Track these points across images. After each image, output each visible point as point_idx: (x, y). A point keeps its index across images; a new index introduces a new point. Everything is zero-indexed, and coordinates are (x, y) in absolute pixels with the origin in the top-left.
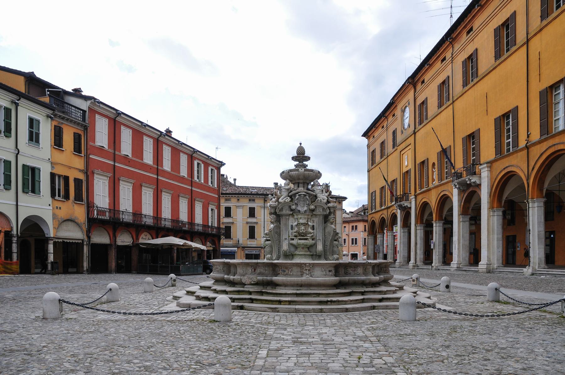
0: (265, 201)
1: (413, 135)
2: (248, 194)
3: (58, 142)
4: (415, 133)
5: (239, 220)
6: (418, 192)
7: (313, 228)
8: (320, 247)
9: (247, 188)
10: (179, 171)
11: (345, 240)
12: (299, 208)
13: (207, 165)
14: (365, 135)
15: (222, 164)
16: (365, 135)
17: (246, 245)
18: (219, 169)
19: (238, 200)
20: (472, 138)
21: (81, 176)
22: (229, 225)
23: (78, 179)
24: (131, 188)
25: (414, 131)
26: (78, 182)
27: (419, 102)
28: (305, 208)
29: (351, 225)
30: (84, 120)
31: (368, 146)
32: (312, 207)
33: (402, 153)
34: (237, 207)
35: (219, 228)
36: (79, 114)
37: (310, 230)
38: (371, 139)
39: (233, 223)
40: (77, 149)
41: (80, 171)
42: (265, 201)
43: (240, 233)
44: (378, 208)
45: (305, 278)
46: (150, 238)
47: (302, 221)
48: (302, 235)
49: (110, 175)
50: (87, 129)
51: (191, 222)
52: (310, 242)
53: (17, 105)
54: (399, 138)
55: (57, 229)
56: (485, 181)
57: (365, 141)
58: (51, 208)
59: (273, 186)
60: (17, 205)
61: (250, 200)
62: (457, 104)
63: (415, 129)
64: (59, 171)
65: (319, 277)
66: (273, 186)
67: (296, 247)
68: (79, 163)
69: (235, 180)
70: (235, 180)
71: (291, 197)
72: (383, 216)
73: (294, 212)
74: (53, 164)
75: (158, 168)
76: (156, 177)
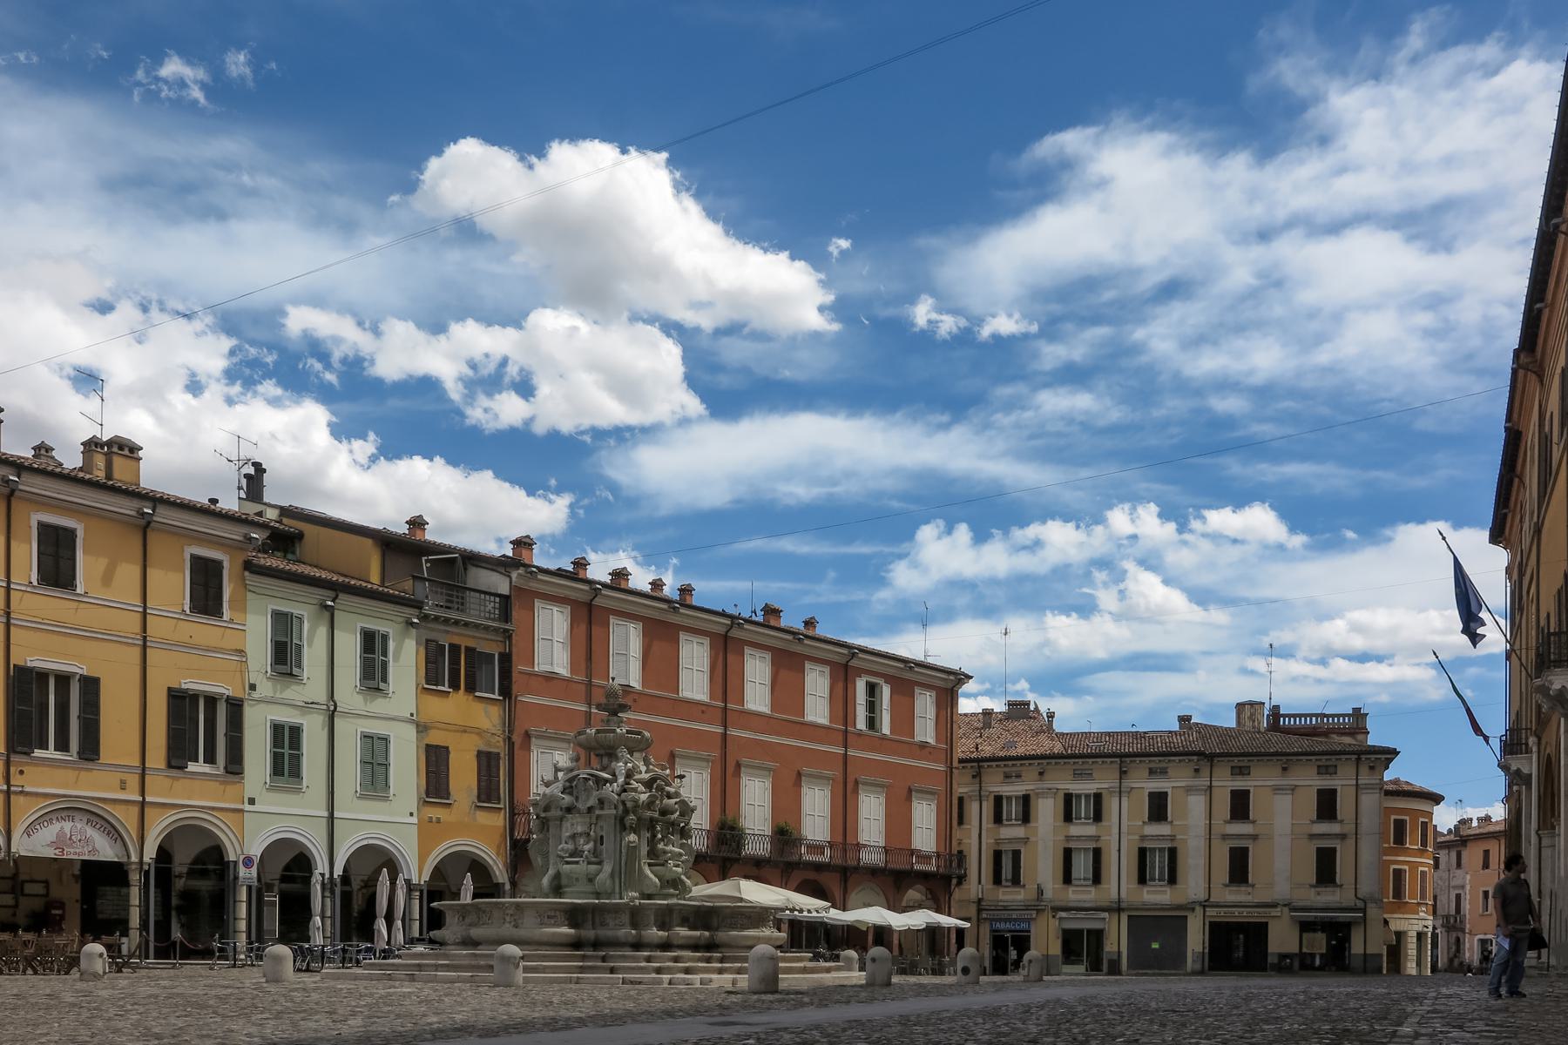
0: (1123, 773)
9: (1137, 736)
19: (1041, 774)
23: (489, 754)
26: (487, 761)
35: (951, 855)
36: (492, 605)
42: (1123, 773)
50: (510, 637)
53: (331, 610)
58: (414, 820)
60: (331, 817)
64: (436, 738)
75: (725, 708)
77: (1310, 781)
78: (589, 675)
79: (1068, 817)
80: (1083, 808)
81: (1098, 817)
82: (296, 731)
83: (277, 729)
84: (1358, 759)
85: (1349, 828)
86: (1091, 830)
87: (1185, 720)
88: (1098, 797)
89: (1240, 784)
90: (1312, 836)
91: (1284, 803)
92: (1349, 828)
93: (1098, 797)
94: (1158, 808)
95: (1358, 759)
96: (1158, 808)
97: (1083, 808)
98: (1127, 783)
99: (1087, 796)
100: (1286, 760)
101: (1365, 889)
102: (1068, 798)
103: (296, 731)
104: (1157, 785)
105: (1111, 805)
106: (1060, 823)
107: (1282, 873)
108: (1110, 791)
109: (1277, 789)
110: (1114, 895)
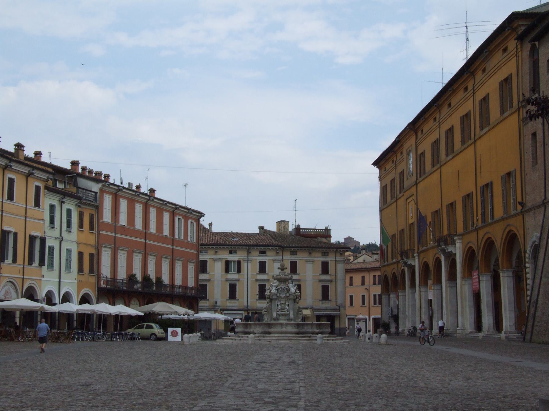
0: (249, 253)
1: (415, 187)
2: (229, 245)
3: (81, 225)
4: (416, 184)
5: (217, 276)
6: (421, 250)
7: (288, 305)
8: (292, 316)
10: (162, 233)
11: (363, 296)
12: (281, 295)
13: (186, 219)
14: (376, 163)
15: (201, 215)
16: (376, 163)
17: (225, 308)
18: (198, 221)
19: (216, 252)
20: (452, 206)
21: (94, 251)
22: (205, 283)
24: (126, 255)
25: (416, 181)
26: (91, 256)
27: (419, 152)
28: (284, 295)
29: (372, 274)
30: (96, 200)
31: (381, 178)
32: (288, 295)
33: (408, 201)
34: (214, 260)
37: (287, 307)
38: (383, 170)
39: (209, 280)
40: (92, 228)
41: (92, 246)
42: (249, 253)
43: (217, 292)
44: (390, 261)
45: (284, 329)
46: (138, 303)
47: (282, 302)
48: (283, 309)
49: (112, 246)
51: (173, 286)
52: (287, 312)
54: (407, 184)
55: (9, 289)
56: (458, 250)
57: (376, 171)
59: (257, 231)
61: (231, 252)
62: (444, 169)
63: (417, 179)
65: (290, 329)
66: (257, 231)
67: (279, 315)
68: (92, 239)
69: (210, 225)
70: (210, 225)
71: (277, 290)
72: (394, 271)
73: (279, 298)
74: (78, 244)
76: (144, 241)
77: (319, 258)
78: (115, 222)
79: (227, 270)
80: (233, 267)
81: (239, 271)
82: (53, 248)
83: (67, 250)
84: (337, 250)
85: (333, 278)
86: (236, 276)
87: (261, 228)
88: (239, 263)
89: (293, 259)
90: (320, 281)
91: (309, 266)
92: (333, 278)
93: (239, 263)
94: (262, 268)
95: (337, 250)
96: (262, 268)
97: (233, 267)
98: (250, 257)
99: (234, 262)
100: (310, 249)
101: (339, 302)
102: (227, 263)
103: (71, 251)
104: (262, 258)
105: (244, 266)
106: (224, 273)
107: (311, 295)
108: (244, 260)
109: (307, 261)
110: (245, 304)
